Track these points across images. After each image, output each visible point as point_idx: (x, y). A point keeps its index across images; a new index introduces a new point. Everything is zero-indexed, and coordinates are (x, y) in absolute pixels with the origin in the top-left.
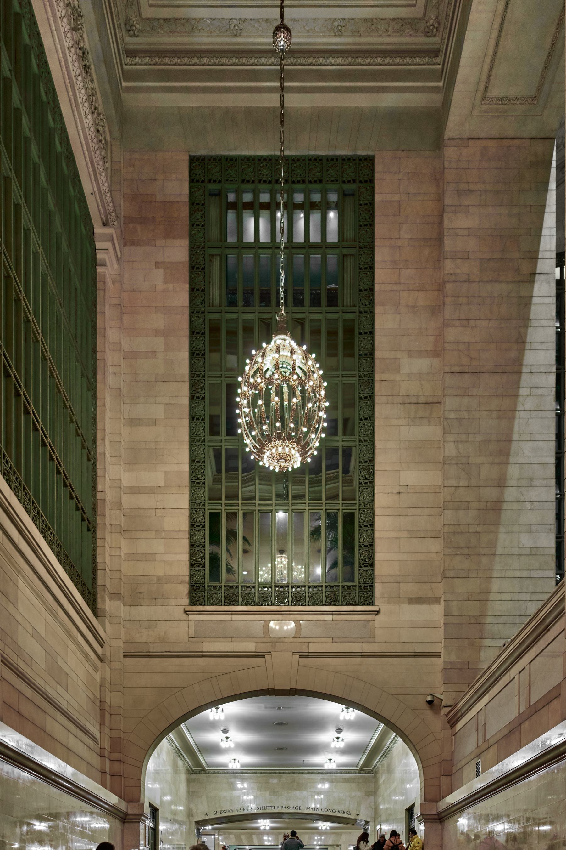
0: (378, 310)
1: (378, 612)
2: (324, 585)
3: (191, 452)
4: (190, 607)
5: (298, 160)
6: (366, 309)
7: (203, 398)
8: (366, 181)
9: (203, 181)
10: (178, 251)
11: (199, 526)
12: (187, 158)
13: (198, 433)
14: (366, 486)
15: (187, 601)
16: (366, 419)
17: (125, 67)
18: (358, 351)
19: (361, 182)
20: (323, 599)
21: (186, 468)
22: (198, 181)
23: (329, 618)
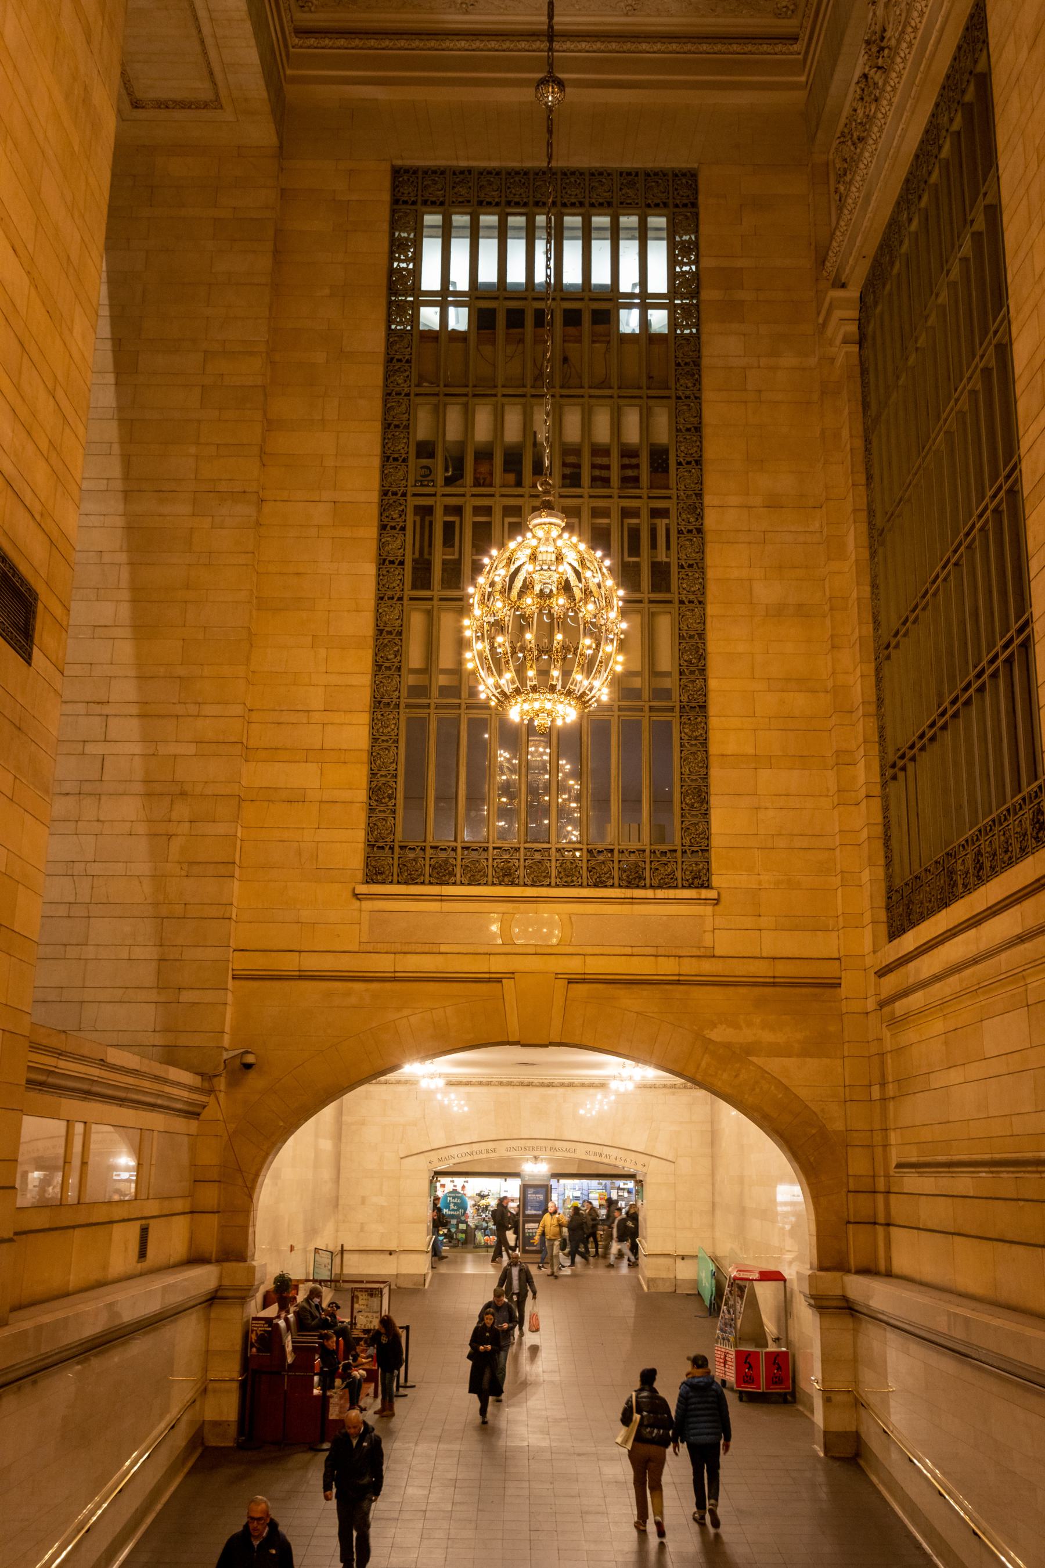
2: (616, 848)
4: (365, 886)
5: (573, 173)
6: (688, 393)
7: (403, 529)
8: (685, 205)
9: (414, 203)
11: (387, 741)
12: (389, 168)
13: (391, 586)
14: (692, 677)
15: (360, 876)
16: (690, 566)
17: (291, 50)
18: (675, 458)
19: (676, 206)
20: (616, 874)
22: (405, 202)
23: (626, 909)
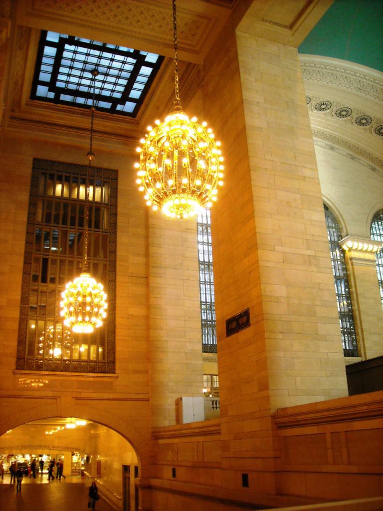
0: (119, 234)
1: (117, 377)
3: (22, 289)
10: (24, 197)
15: (14, 367)
21: (19, 297)
23: (92, 379)
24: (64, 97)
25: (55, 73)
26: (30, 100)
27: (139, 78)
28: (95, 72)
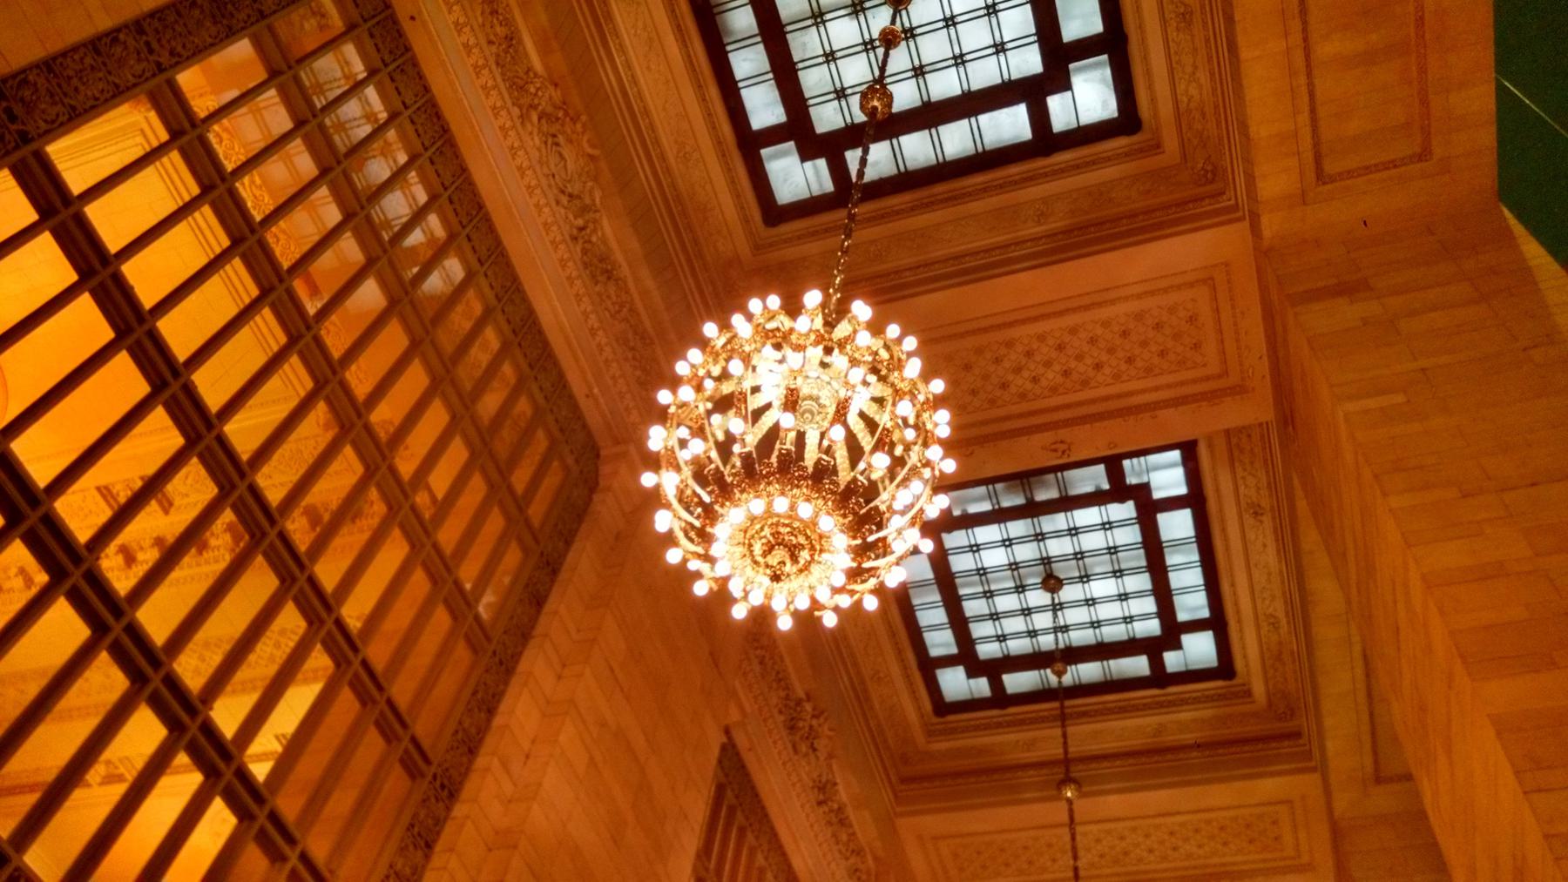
24: (1016, 682)
25: (959, 623)
26: (935, 720)
27: (1172, 559)
28: (1052, 583)
